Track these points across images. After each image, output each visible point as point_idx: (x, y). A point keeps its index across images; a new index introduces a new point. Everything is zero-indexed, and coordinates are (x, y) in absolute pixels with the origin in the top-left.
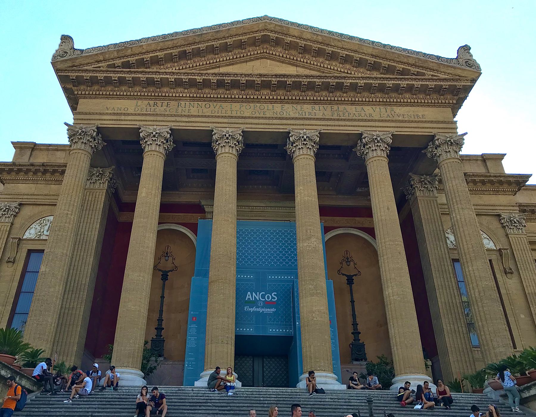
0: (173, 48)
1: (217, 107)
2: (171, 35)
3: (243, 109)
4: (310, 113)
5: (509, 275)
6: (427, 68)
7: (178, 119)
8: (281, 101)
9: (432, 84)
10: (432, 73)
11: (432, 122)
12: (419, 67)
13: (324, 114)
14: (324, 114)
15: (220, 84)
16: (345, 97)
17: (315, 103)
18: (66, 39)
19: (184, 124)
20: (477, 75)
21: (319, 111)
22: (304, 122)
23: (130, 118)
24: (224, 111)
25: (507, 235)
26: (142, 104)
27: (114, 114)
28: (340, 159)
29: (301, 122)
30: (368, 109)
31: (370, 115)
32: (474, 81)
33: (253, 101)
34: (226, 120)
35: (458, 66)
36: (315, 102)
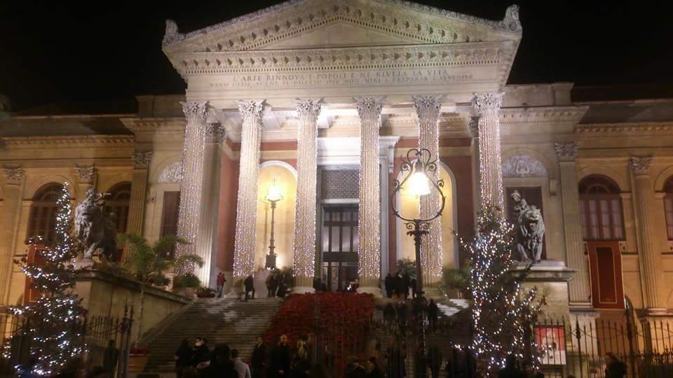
3: (320, 78)
31: (426, 79)
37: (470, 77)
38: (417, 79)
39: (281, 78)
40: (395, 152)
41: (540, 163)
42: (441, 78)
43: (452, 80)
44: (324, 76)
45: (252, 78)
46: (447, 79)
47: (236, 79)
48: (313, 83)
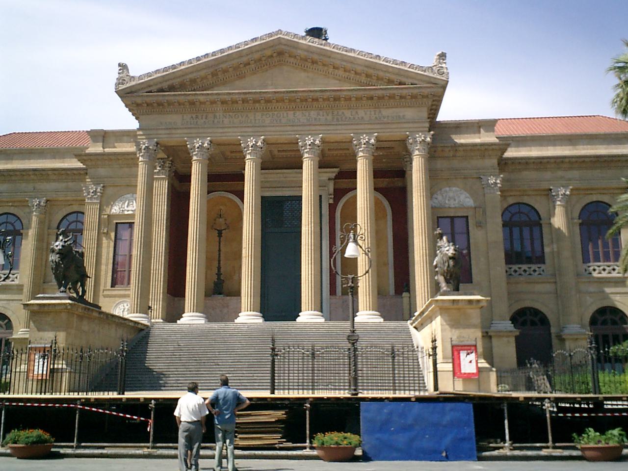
1: (244, 117)
3: (264, 117)
4: (315, 119)
5: (480, 228)
11: (409, 122)
13: (326, 119)
14: (326, 119)
17: (321, 110)
18: (123, 67)
19: (219, 135)
20: (445, 82)
23: (179, 131)
24: (249, 121)
25: (484, 195)
27: (167, 129)
29: (308, 128)
30: (361, 113)
31: (362, 118)
32: (444, 87)
35: (431, 75)
37: (404, 116)
38: (354, 119)
39: (228, 116)
41: (468, 195)
42: (376, 118)
43: (385, 120)
44: (268, 116)
46: (382, 119)
48: (257, 121)
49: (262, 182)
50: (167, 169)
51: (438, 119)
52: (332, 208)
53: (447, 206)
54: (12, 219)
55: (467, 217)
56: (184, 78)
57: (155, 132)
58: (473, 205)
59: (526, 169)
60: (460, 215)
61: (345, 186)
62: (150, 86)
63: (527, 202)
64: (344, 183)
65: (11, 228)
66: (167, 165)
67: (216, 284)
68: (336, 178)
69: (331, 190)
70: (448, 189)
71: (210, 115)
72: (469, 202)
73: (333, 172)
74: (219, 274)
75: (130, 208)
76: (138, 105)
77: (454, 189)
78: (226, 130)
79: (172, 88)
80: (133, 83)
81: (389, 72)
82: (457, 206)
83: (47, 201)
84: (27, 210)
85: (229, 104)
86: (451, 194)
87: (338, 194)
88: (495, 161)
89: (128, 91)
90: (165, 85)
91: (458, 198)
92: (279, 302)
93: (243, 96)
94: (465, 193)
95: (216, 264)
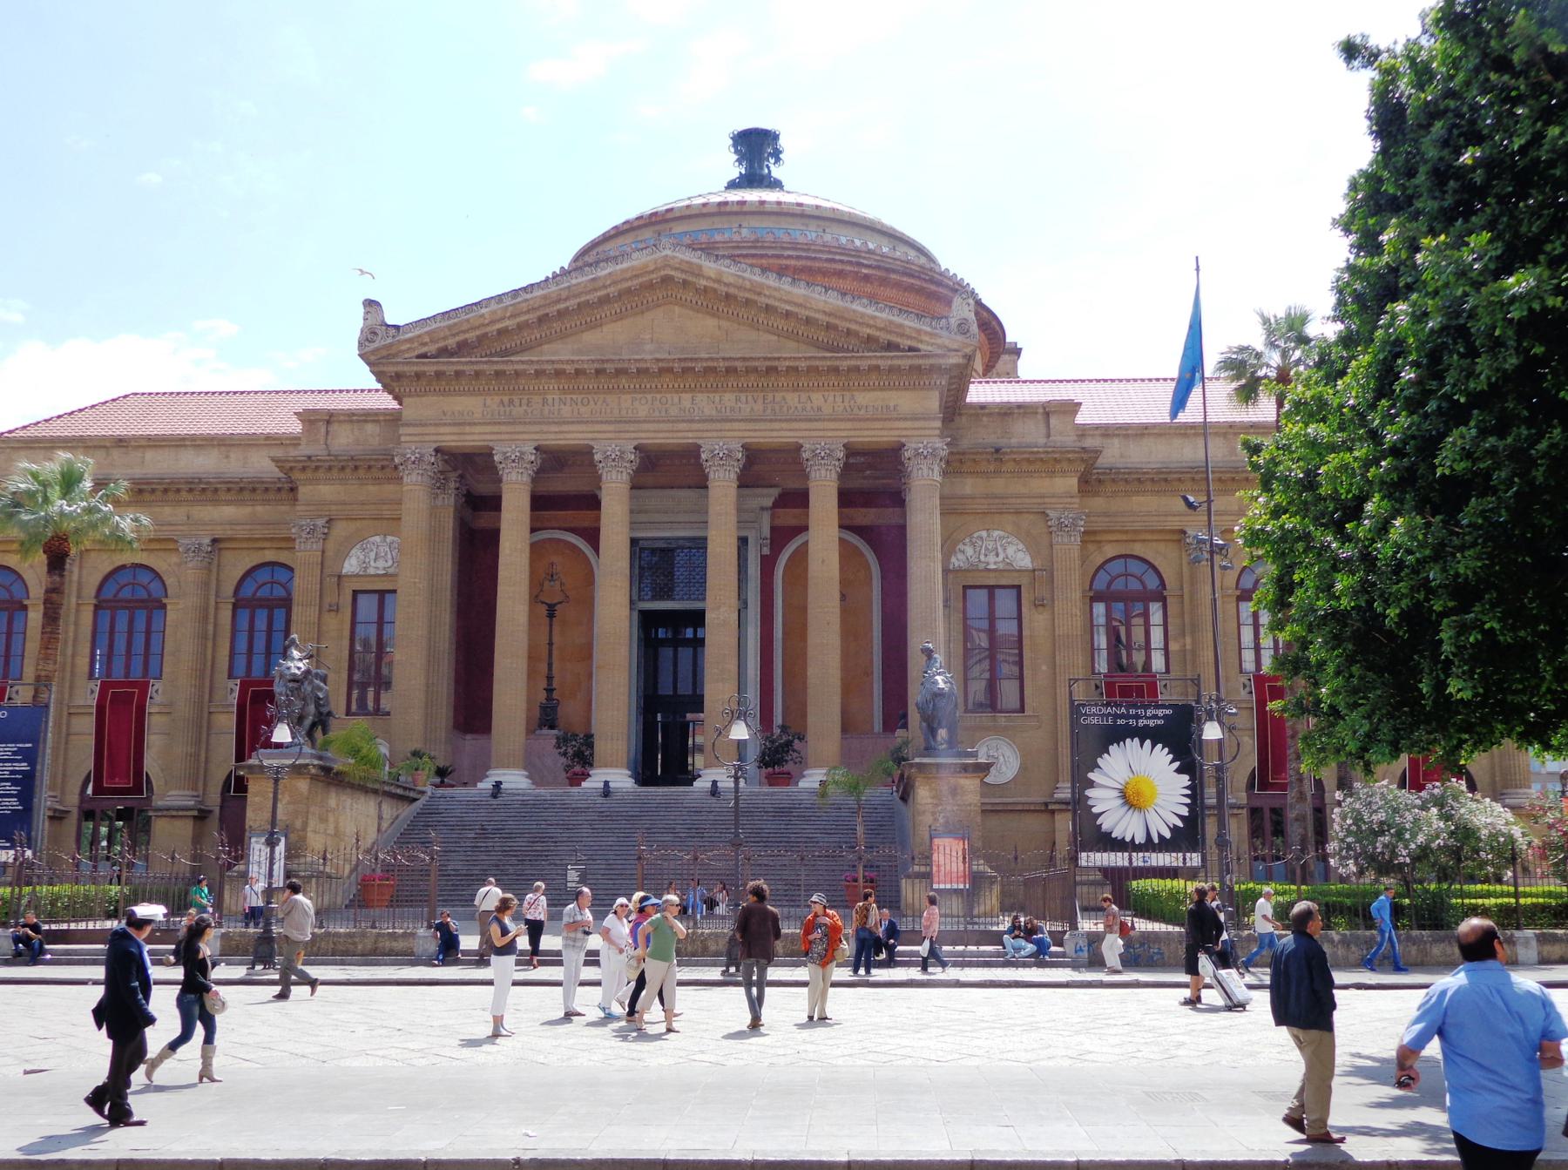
0: (528, 312)
2: (524, 289)
3: (637, 404)
4: (732, 410)
6: (902, 335)
7: (545, 428)
8: (691, 390)
9: (905, 363)
10: (909, 343)
11: (905, 419)
12: (890, 332)
15: (598, 372)
16: (783, 381)
18: (371, 305)
21: (747, 404)
22: (720, 427)
23: (478, 429)
26: (493, 402)
27: (455, 424)
28: (772, 475)
29: (718, 426)
30: (817, 398)
31: (819, 409)
33: (651, 390)
34: (611, 427)
36: (741, 390)
38: (804, 409)
40: (773, 517)
41: (1021, 546)
45: (517, 402)
47: (489, 401)
48: (624, 413)
49: (632, 512)
50: (452, 492)
51: (968, 400)
52: (768, 565)
53: (982, 566)
54: (144, 578)
55: (1018, 587)
56: (488, 329)
57: (432, 430)
58: (1030, 566)
59: (1138, 493)
60: (1003, 582)
61: (793, 522)
62: (425, 344)
63: (1141, 555)
64: (788, 517)
65: (144, 595)
66: (452, 485)
67: (544, 708)
68: (776, 505)
69: (766, 532)
70: (984, 534)
71: (537, 399)
72: (1024, 561)
73: (767, 497)
74: (549, 690)
75: (381, 563)
76: (398, 376)
77: (996, 533)
78: (565, 428)
79: (463, 348)
80: (389, 340)
81: (869, 326)
82: (1001, 566)
83: (215, 541)
84: (174, 559)
85: (571, 377)
86: (991, 545)
87: (781, 536)
88: (1072, 483)
89: (384, 353)
90: (451, 342)
91: (1004, 551)
92: (665, 751)
93: (596, 365)
94: (1015, 541)
95: (544, 667)
